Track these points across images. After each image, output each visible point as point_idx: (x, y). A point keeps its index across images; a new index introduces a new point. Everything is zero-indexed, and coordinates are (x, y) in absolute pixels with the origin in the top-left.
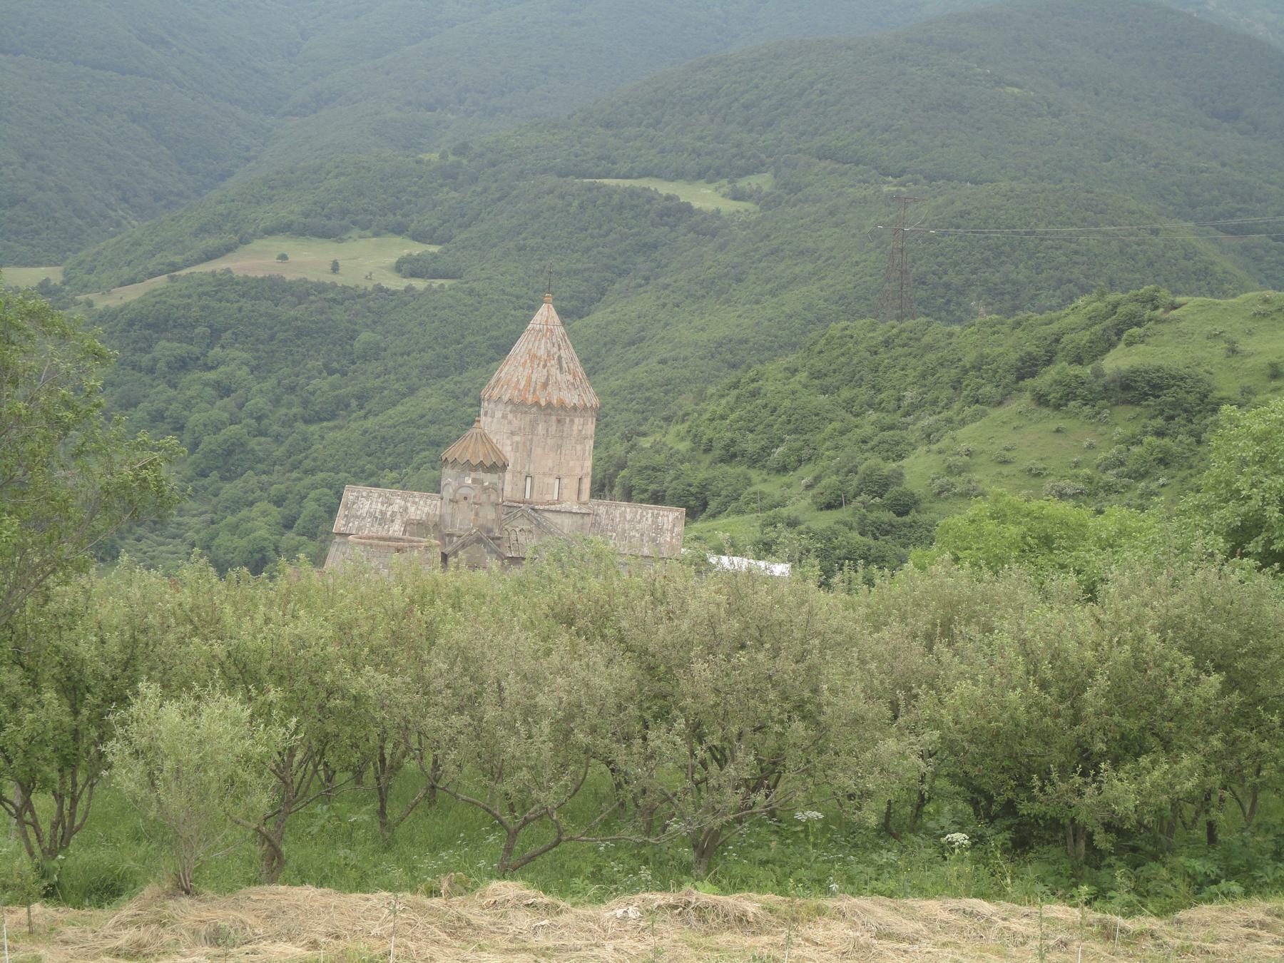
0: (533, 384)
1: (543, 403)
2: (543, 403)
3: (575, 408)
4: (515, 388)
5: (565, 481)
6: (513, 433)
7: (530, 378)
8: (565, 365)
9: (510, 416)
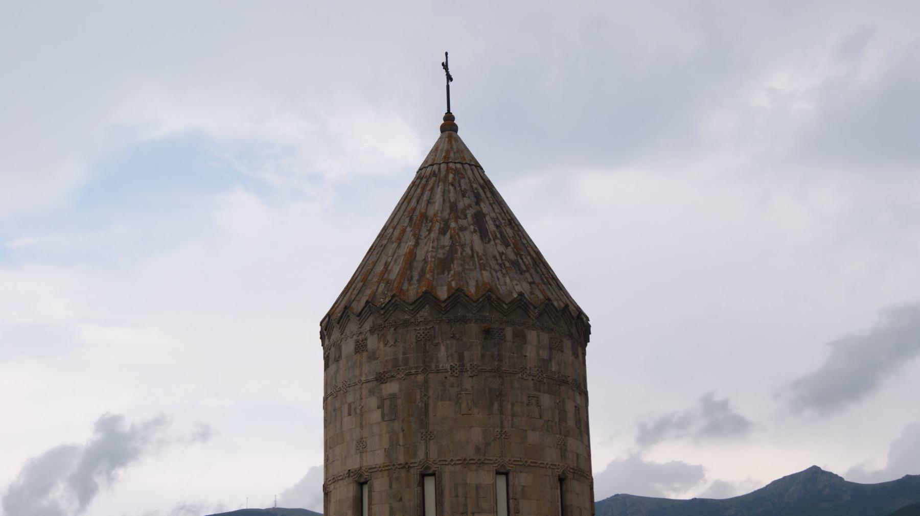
0: (418, 266)
1: (443, 293)
2: (443, 293)
4: (382, 277)
5: (522, 479)
6: (381, 378)
7: (412, 254)
8: (491, 227)
9: (372, 342)
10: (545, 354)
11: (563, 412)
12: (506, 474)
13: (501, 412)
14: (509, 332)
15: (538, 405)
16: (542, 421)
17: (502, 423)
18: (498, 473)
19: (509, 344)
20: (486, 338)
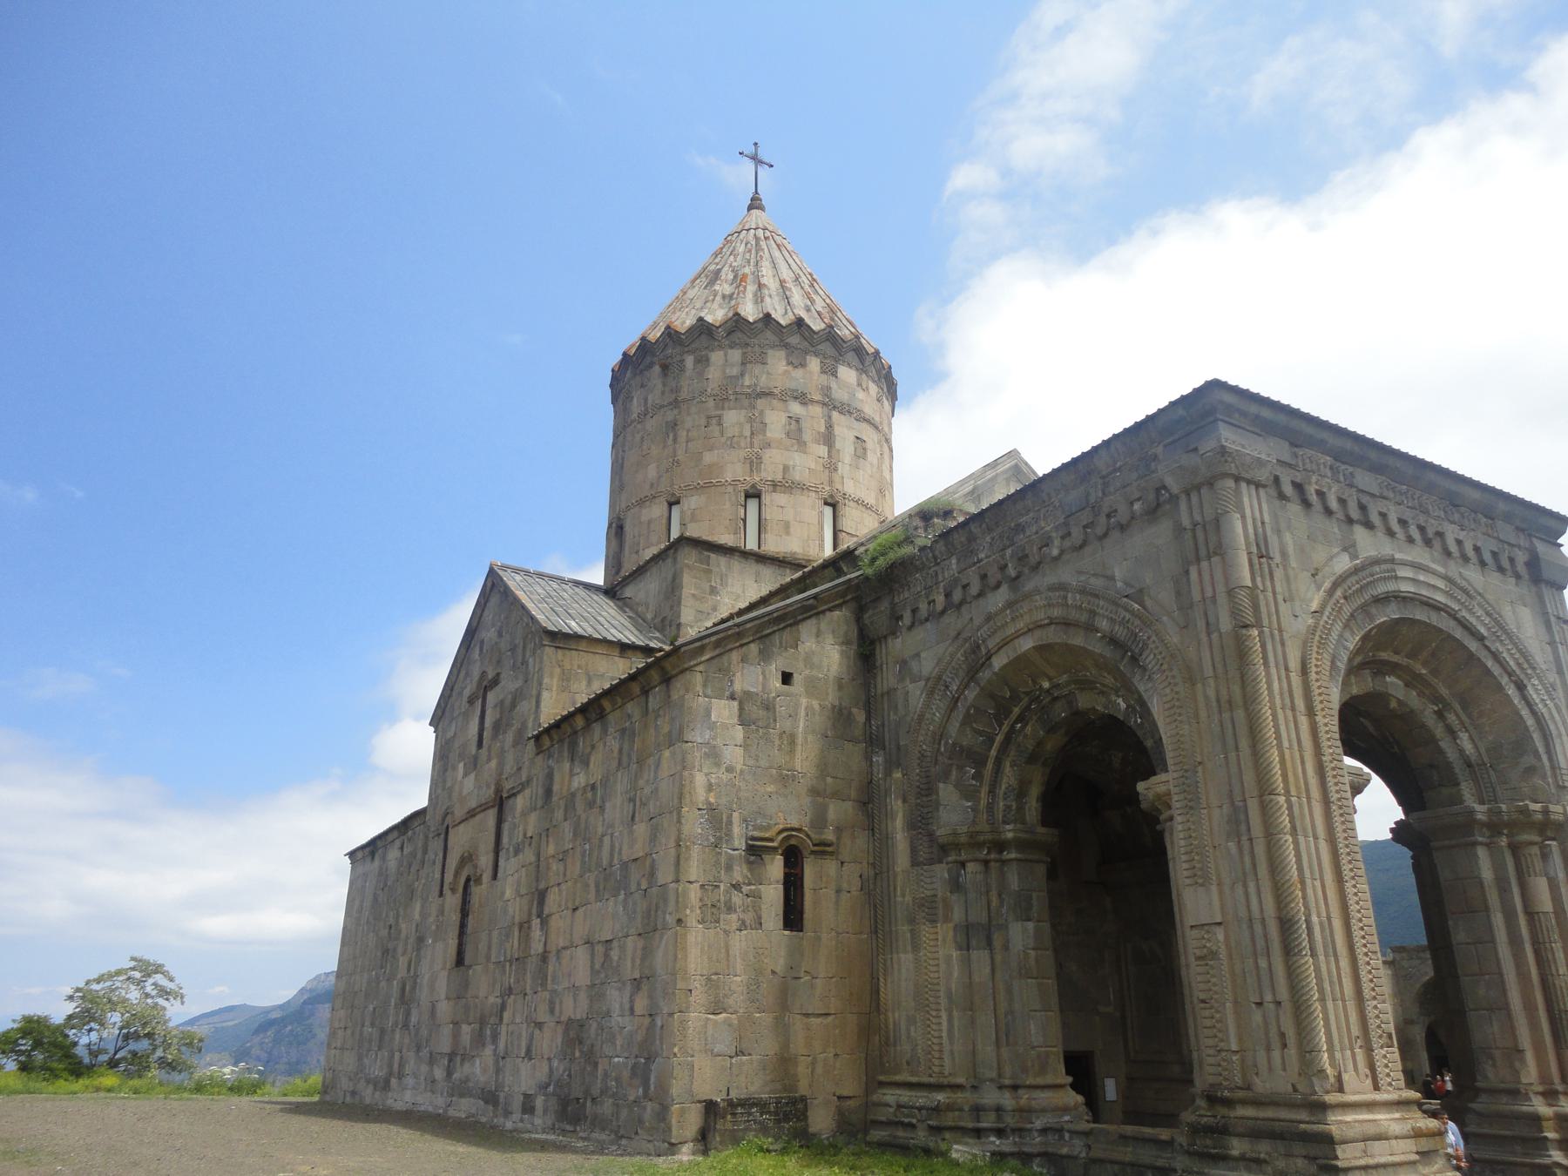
3: (702, 328)
12: (678, 502)
13: (675, 440)
14: (689, 361)
15: (720, 424)
16: (723, 440)
17: (675, 451)
18: (671, 504)
19: (688, 374)
20: (665, 375)
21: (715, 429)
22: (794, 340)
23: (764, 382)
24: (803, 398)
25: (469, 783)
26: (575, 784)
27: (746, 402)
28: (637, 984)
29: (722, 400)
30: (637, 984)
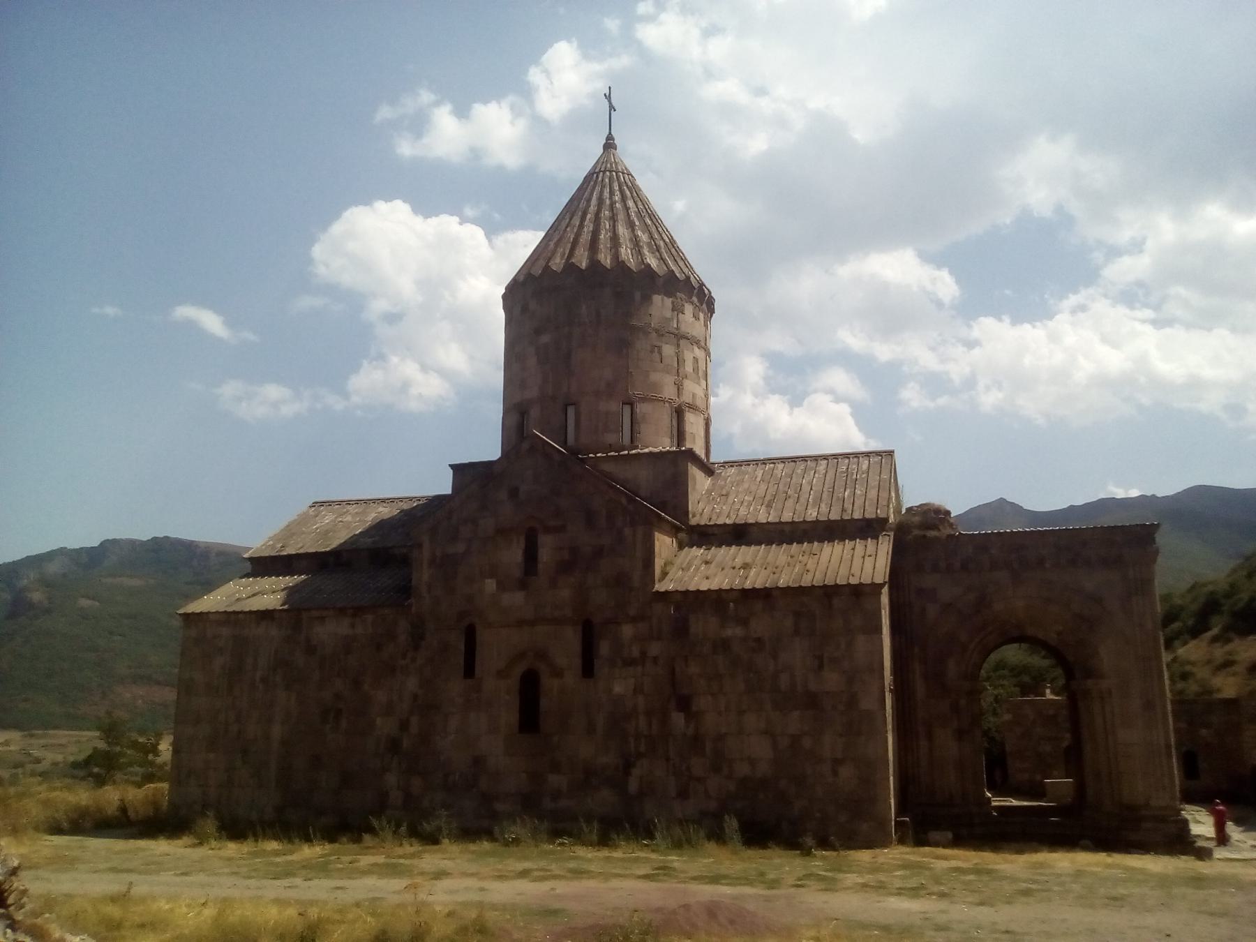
5: (641, 408)
6: (538, 332)
10: (668, 314)
11: (680, 361)
14: (638, 295)
15: (660, 353)
21: (656, 355)
22: (695, 299)
23: (684, 329)
24: (697, 343)
25: (515, 599)
26: (729, 632)
27: (675, 341)
28: (837, 762)
29: (660, 334)
30: (837, 762)
